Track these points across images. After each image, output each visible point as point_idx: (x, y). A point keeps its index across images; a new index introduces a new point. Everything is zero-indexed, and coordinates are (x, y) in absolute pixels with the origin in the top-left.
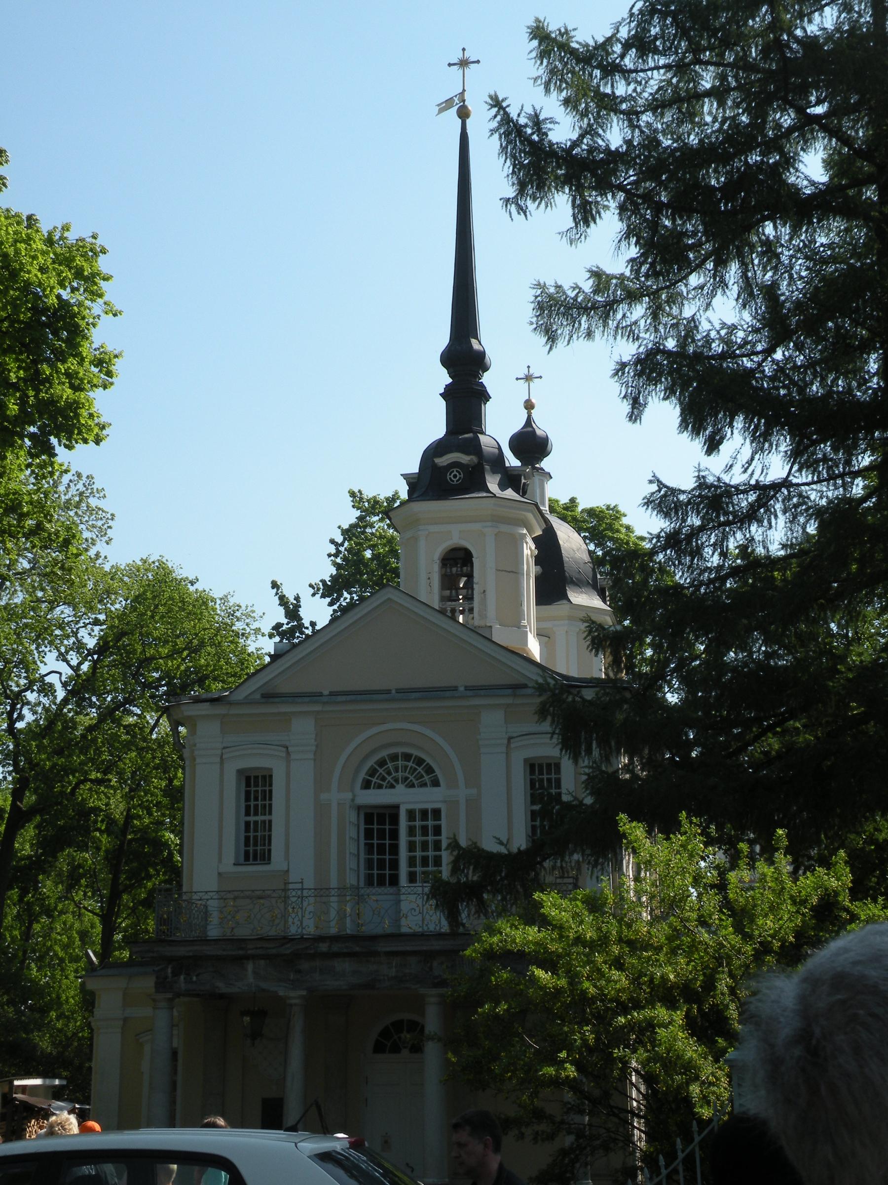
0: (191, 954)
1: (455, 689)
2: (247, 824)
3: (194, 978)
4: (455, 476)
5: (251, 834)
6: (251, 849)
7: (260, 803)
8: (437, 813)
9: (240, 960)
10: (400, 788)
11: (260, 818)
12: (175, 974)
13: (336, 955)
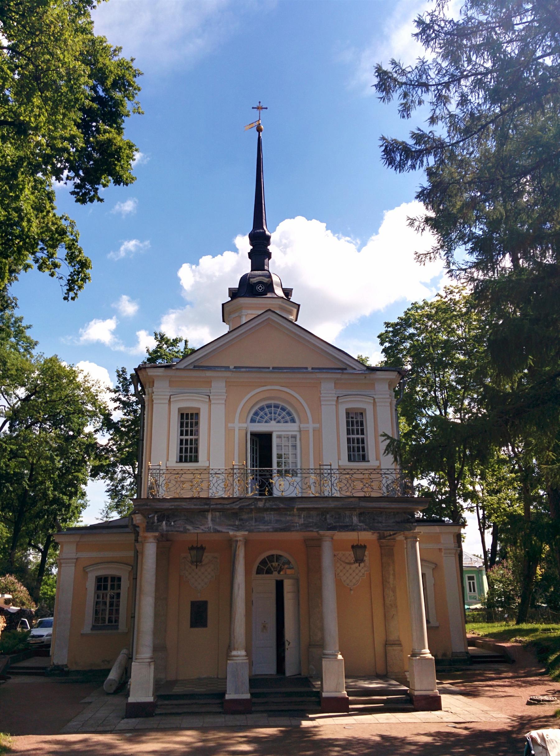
0: (173, 507)
1: (307, 368)
2: (181, 441)
3: (173, 523)
4: (260, 288)
5: (184, 446)
6: (184, 454)
7: (189, 429)
8: (294, 437)
9: (203, 513)
10: (273, 422)
11: (189, 437)
12: (160, 520)
13: (265, 510)
